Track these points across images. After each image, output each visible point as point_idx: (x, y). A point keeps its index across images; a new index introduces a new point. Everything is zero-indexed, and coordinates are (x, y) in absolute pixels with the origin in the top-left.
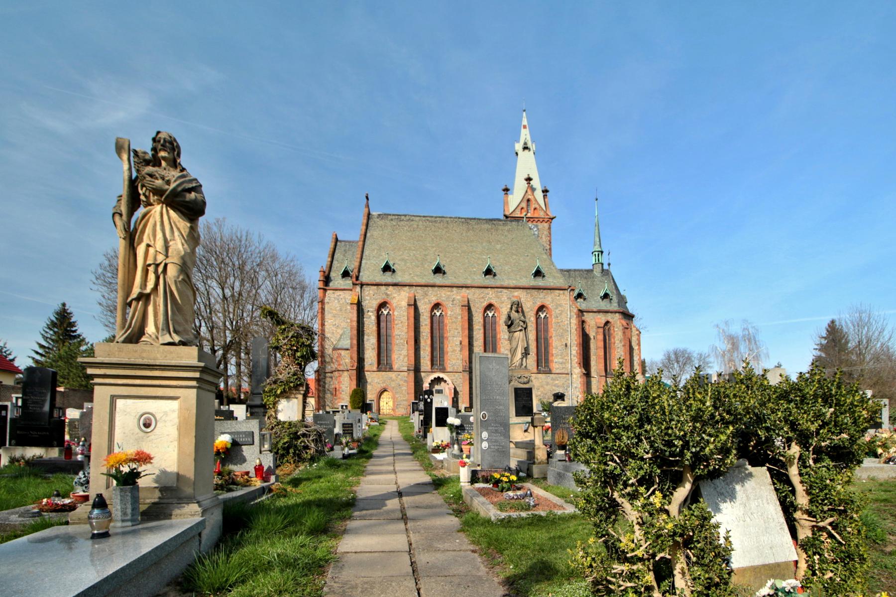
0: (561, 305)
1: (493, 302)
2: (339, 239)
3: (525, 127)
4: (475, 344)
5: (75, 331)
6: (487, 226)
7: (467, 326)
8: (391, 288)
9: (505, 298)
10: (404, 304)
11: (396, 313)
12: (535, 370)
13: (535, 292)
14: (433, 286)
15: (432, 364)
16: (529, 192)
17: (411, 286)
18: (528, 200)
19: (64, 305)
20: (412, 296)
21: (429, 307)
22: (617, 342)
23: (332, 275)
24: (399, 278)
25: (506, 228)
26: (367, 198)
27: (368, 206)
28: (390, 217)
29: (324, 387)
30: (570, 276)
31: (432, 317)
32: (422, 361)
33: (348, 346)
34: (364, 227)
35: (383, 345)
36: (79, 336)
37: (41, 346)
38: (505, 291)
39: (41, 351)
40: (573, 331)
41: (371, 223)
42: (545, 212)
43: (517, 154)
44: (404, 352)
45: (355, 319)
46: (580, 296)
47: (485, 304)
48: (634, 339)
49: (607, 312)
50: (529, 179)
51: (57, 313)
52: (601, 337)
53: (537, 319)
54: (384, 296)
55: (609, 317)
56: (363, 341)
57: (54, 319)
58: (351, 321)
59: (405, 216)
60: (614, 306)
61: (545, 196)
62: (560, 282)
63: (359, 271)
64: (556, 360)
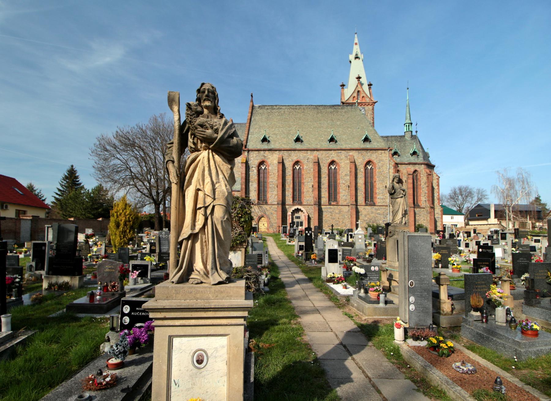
0: (382, 160)
1: (335, 159)
3: (356, 44)
4: (322, 187)
5: (78, 181)
6: (330, 110)
7: (317, 175)
8: (267, 152)
10: (276, 162)
11: (270, 168)
12: (364, 204)
15: (293, 200)
16: (359, 86)
17: (280, 150)
18: (358, 92)
19: (72, 166)
20: (281, 157)
21: (292, 164)
22: (422, 184)
24: (272, 146)
25: (344, 111)
26: (252, 96)
27: (252, 101)
28: (266, 107)
30: (388, 141)
33: (239, 189)
34: (250, 114)
35: (262, 188)
36: (80, 184)
37: (59, 190)
38: (343, 152)
39: (59, 193)
41: (254, 112)
42: (370, 99)
43: (350, 62)
44: (275, 193)
45: (244, 172)
46: (395, 153)
47: (330, 161)
48: (435, 182)
50: (359, 78)
51: (68, 171)
53: (365, 170)
55: (417, 167)
56: (249, 186)
57: (67, 174)
58: (242, 174)
59: (276, 106)
61: (370, 88)
62: (382, 145)
63: (247, 142)
64: (378, 197)
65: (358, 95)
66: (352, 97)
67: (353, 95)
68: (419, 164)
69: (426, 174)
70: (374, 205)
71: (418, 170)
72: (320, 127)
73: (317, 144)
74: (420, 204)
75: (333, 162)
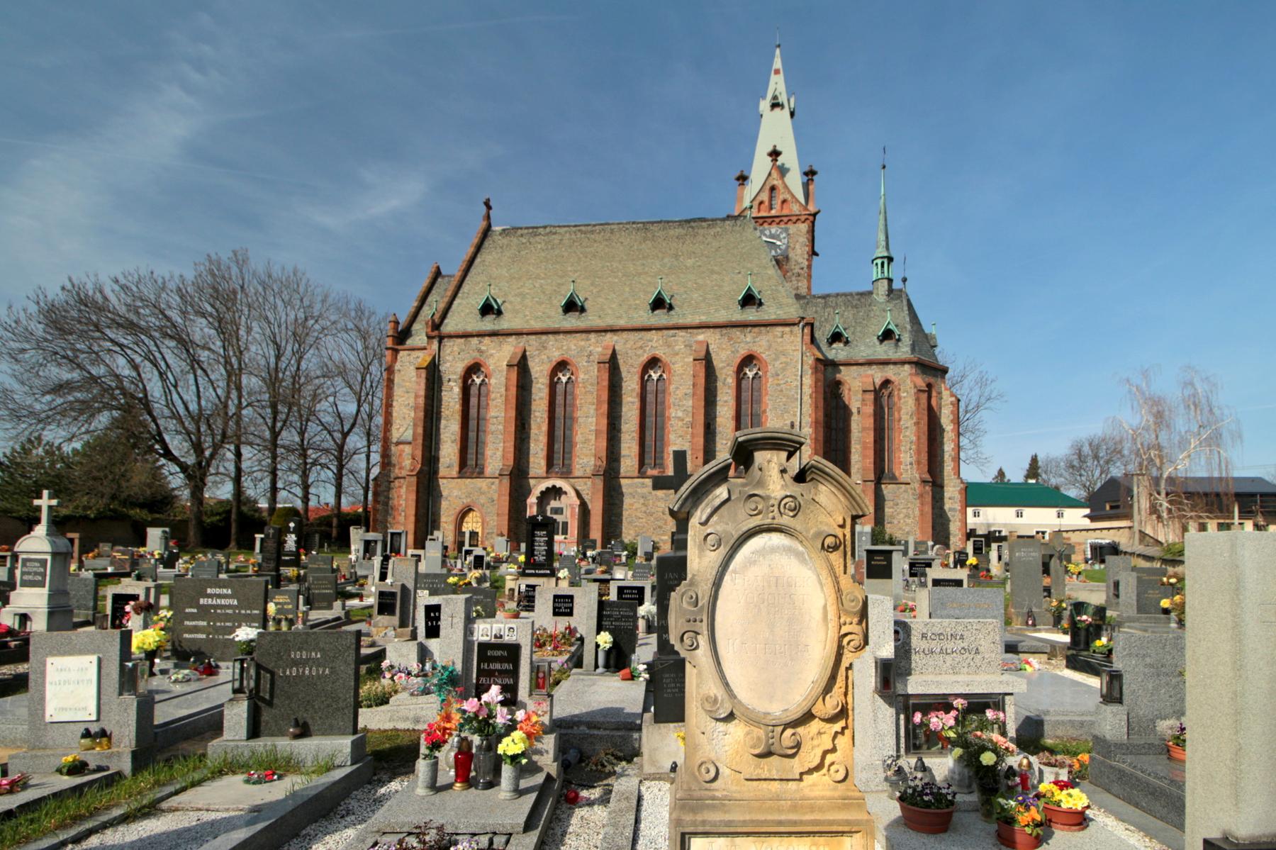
0: (784, 353)
1: (659, 353)
2: (443, 272)
3: (777, 72)
6: (679, 231)
7: (605, 396)
8: (487, 340)
9: (680, 347)
11: (493, 381)
13: (736, 333)
14: (556, 332)
16: (775, 174)
17: (519, 334)
18: (773, 189)
21: (547, 368)
23: (416, 327)
24: (505, 323)
25: (712, 231)
26: (489, 207)
27: (488, 217)
28: (520, 232)
29: (386, 504)
31: (553, 386)
32: (531, 460)
33: (410, 438)
35: (472, 435)
40: (806, 398)
41: (486, 244)
47: (645, 358)
50: (775, 154)
52: (869, 409)
54: (476, 354)
55: (890, 372)
58: (416, 396)
59: (545, 227)
60: (904, 351)
65: (771, 198)
66: (756, 204)
67: (759, 199)
68: (895, 363)
69: (913, 391)
71: (893, 378)
72: (640, 274)
73: (620, 317)
74: (897, 474)
75: (653, 362)
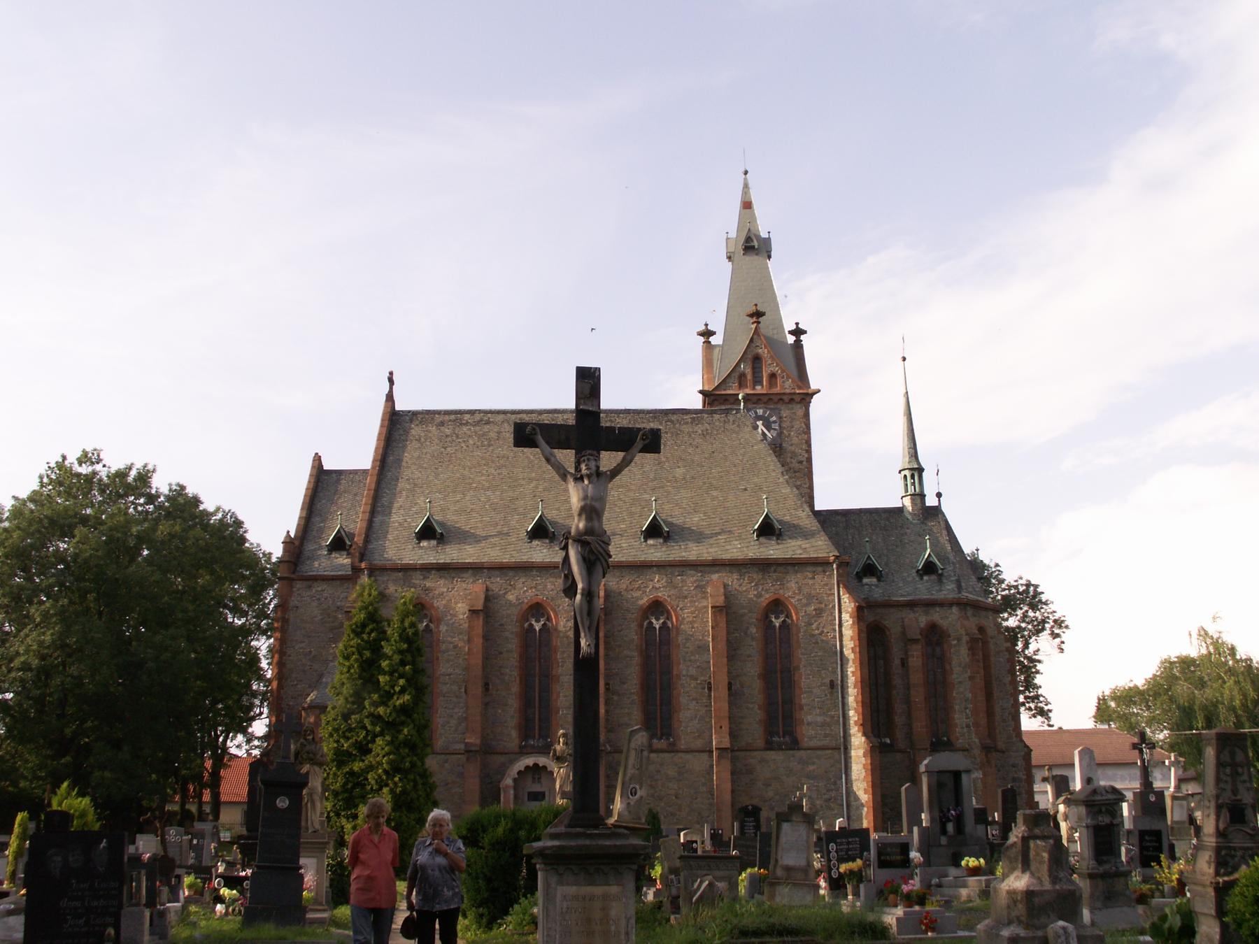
1: (663, 594)
12: (760, 743)
22: (957, 670)
25: (699, 429)
46: (869, 570)
49: (930, 604)
55: (936, 616)
62: (820, 547)
66: (736, 375)
70: (795, 744)
